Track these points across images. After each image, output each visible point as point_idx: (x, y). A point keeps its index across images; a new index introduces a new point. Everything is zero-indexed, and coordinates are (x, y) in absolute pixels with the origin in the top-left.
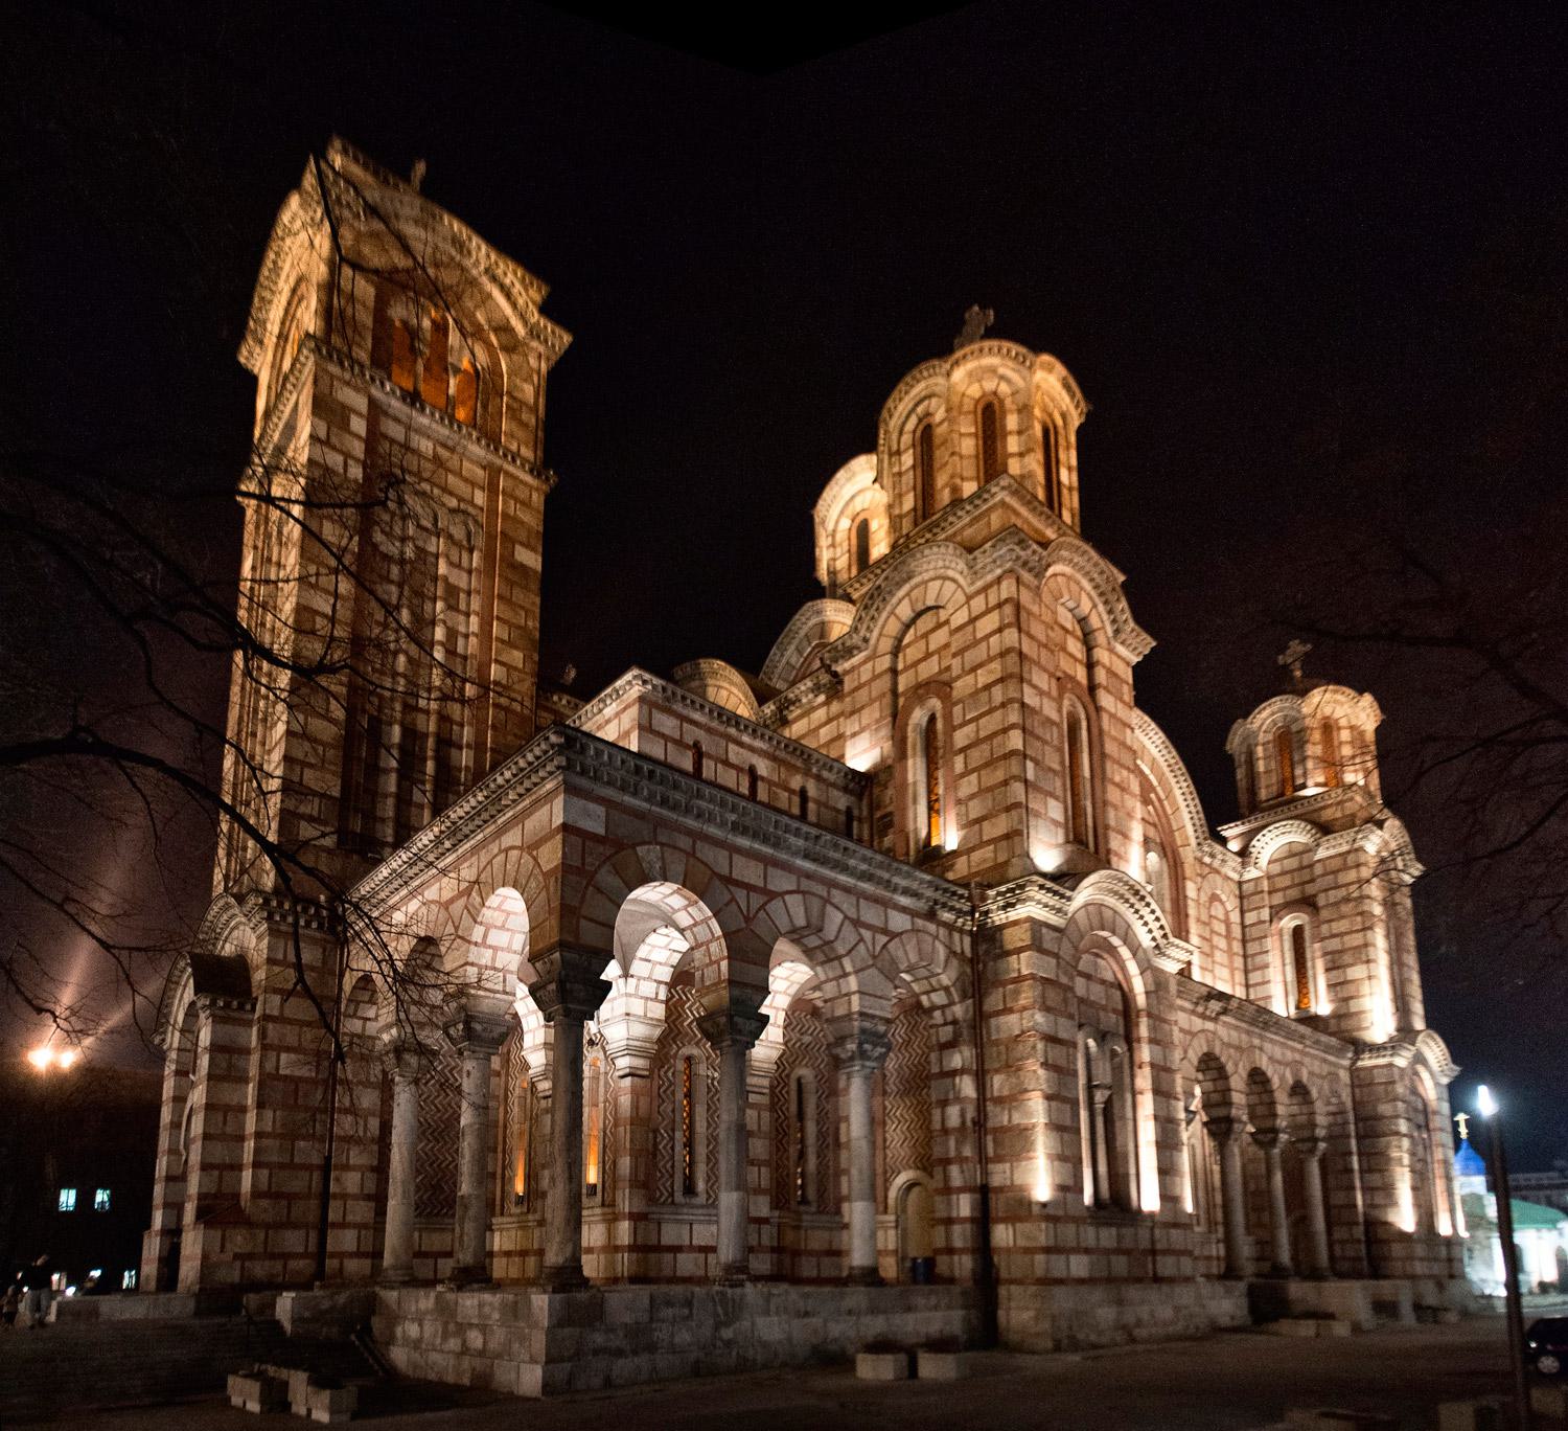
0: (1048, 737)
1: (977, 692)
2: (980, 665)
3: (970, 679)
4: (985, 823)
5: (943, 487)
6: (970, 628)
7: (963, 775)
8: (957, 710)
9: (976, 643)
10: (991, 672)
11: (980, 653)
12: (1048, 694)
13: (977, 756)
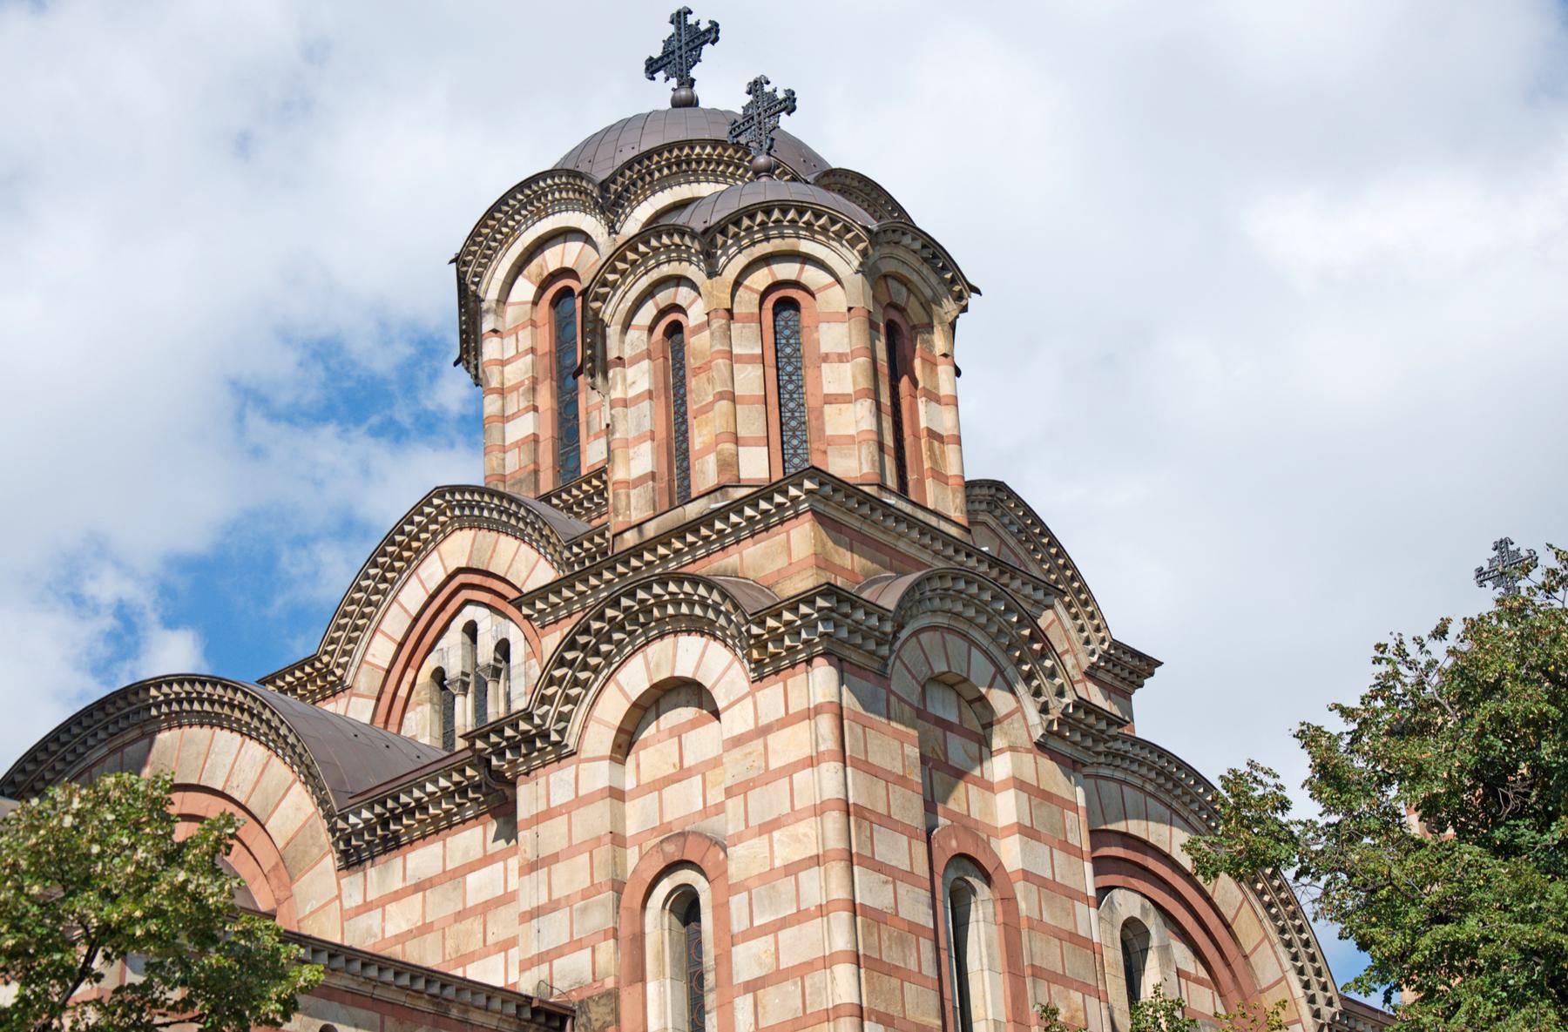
0: (913, 966)
3: (758, 845)
5: (706, 451)
6: (758, 744)
8: (738, 903)
9: (768, 777)
10: (797, 840)
12: (908, 876)
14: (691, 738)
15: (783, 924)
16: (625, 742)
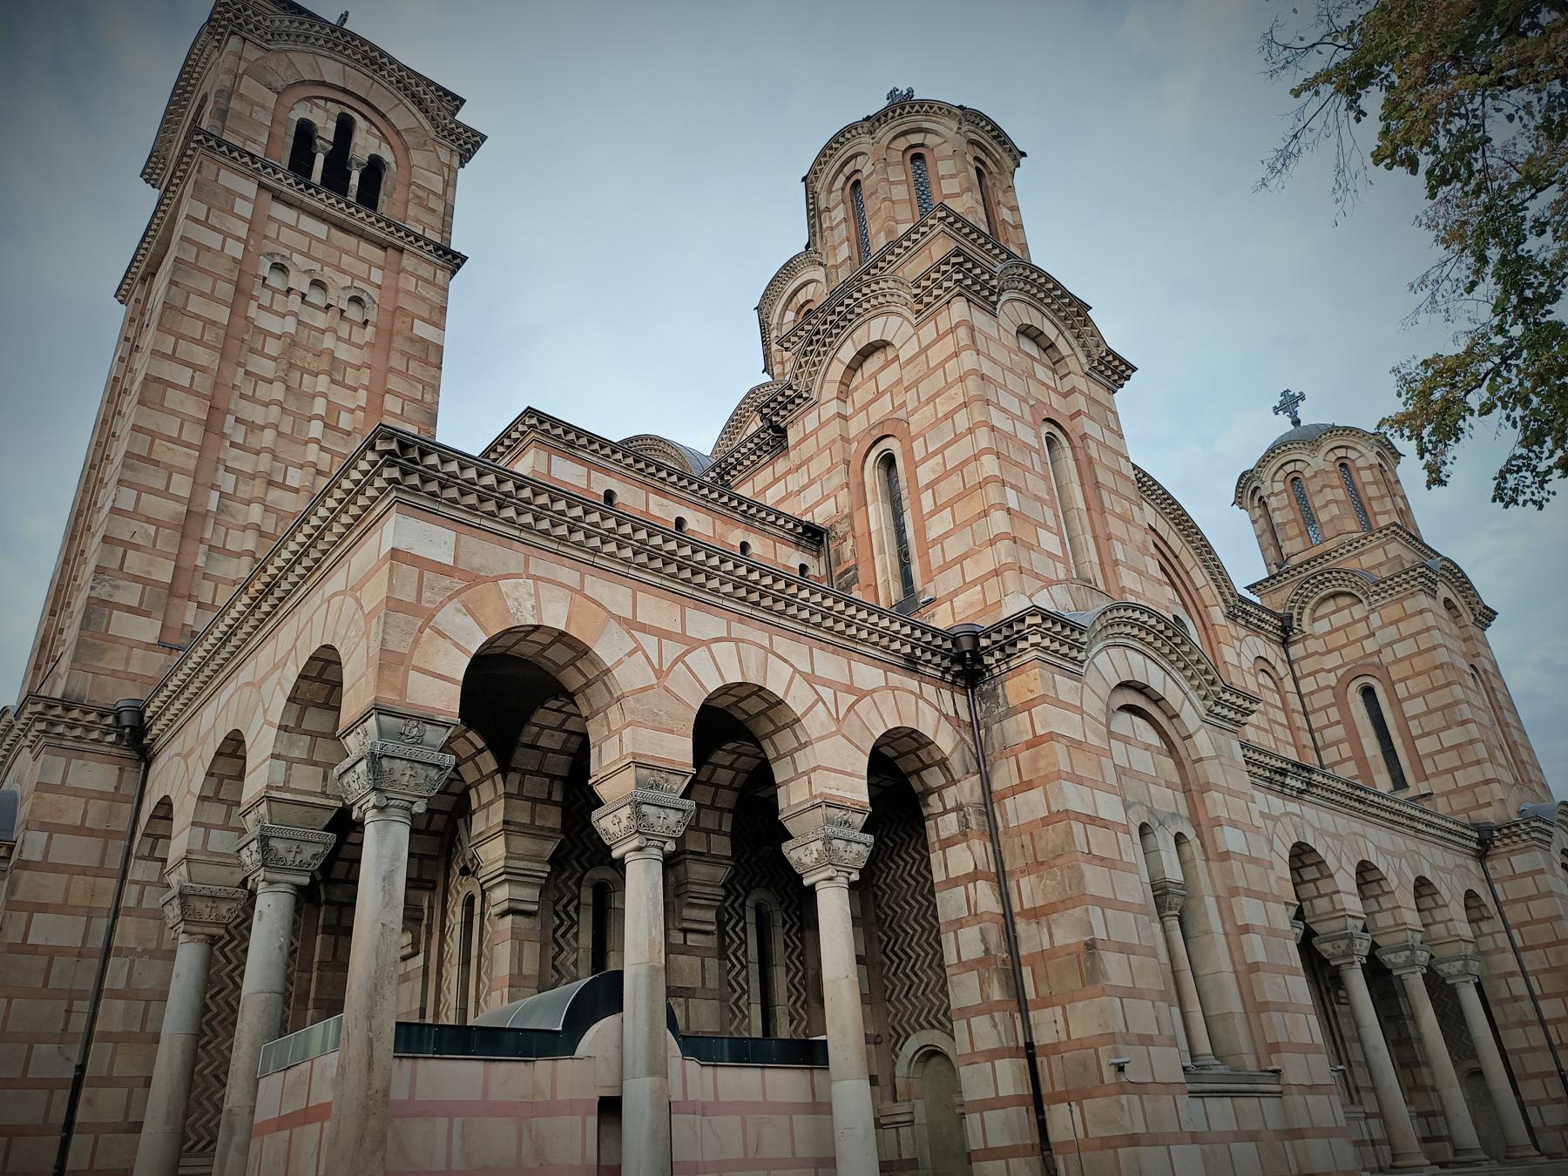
1: (938, 421)
2: (938, 394)
3: (929, 409)
7: (932, 513)
8: (918, 446)
9: (931, 371)
10: (951, 398)
11: (937, 381)
13: (948, 489)
14: (881, 377)
16: (845, 383)
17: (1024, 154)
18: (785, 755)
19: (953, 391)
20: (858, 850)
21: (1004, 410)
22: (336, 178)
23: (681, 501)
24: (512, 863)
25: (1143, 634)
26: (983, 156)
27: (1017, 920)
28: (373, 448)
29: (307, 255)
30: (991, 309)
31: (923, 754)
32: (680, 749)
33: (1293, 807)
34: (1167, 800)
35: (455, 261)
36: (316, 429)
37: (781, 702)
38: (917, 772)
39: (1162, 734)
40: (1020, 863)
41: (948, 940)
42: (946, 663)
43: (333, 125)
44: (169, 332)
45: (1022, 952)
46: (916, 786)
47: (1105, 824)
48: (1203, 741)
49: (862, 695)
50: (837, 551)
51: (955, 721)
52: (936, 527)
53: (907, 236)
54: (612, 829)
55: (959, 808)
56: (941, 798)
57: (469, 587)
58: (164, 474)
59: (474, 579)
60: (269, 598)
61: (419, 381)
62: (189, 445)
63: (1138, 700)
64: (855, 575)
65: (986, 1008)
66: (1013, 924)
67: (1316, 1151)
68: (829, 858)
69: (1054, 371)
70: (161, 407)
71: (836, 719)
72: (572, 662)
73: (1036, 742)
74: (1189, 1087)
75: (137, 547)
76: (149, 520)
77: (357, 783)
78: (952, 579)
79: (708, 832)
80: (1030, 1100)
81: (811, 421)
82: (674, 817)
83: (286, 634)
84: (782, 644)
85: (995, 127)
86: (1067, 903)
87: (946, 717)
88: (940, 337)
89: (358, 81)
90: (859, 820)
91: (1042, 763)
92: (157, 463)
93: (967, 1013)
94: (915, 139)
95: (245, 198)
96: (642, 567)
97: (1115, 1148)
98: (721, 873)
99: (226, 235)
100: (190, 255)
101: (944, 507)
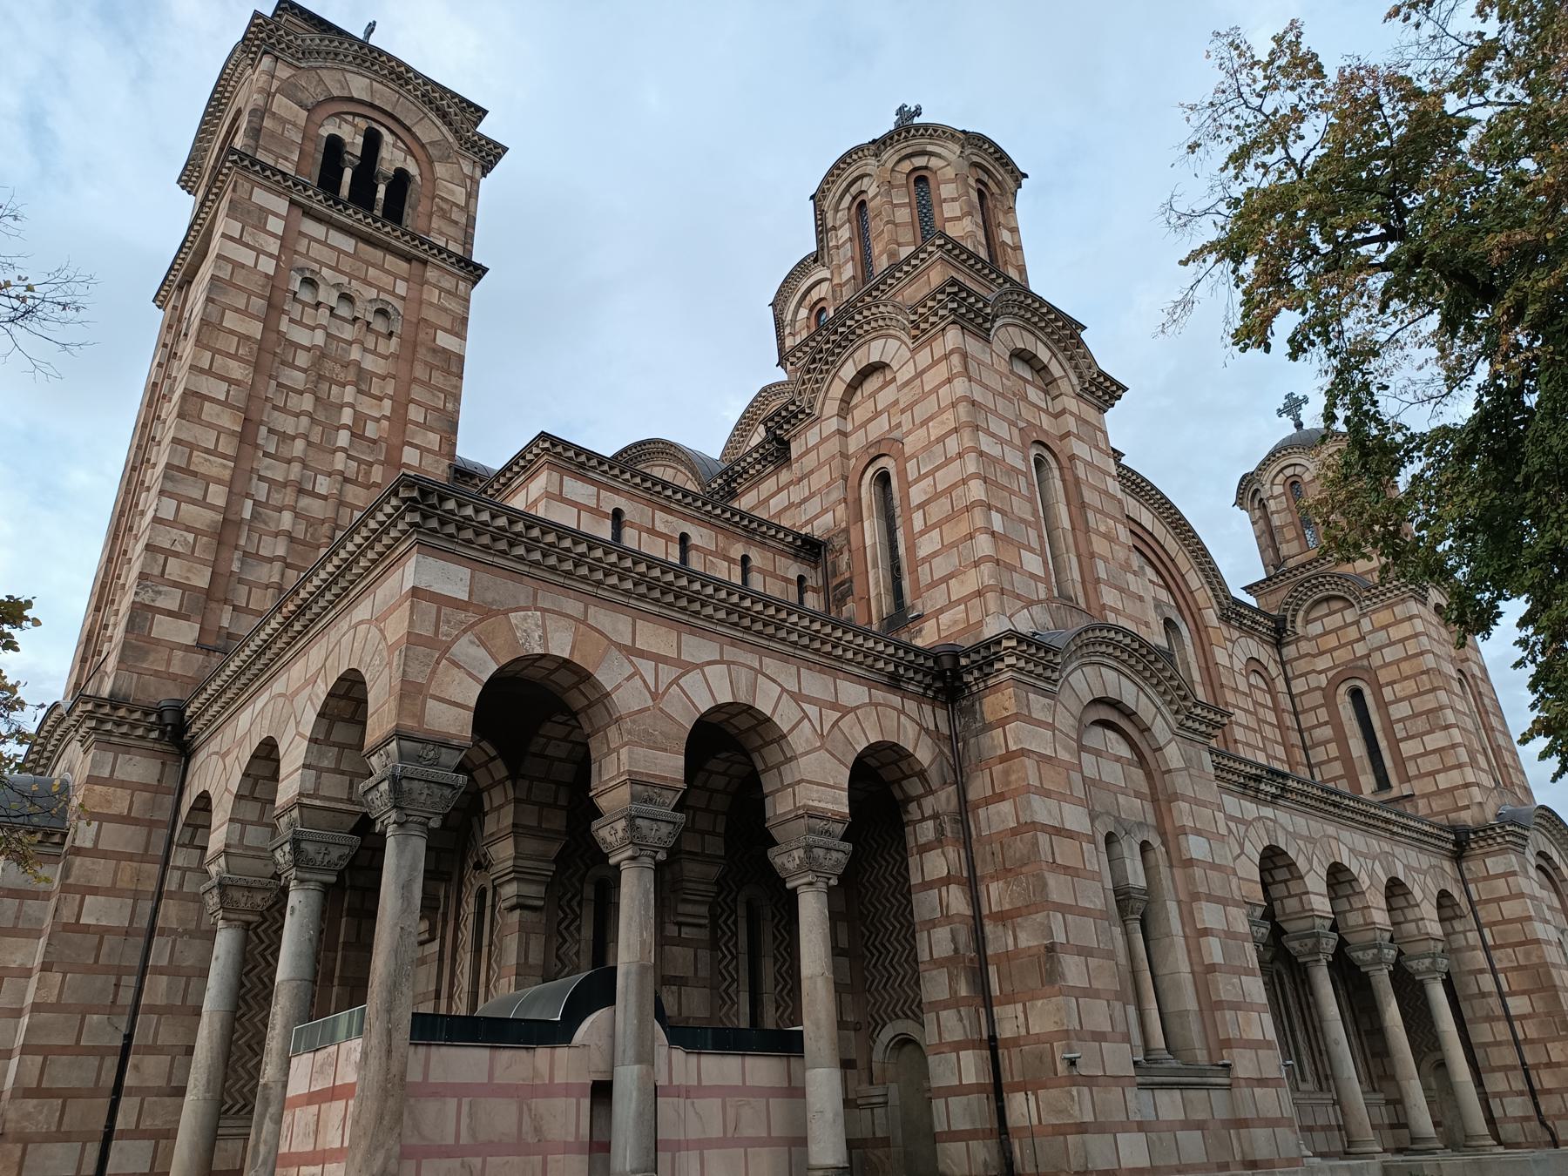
1: (930, 445)
2: (931, 418)
3: (922, 432)
4: (952, 582)
8: (911, 466)
9: (925, 395)
10: (943, 423)
11: (930, 406)
13: (938, 510)
14: (880, 396)
15: (938, 468)
17: (1025, 176)
18: (772, 768)
19: (945, 416)
20: (837, 857)
21: (993, 435)
22: (362, 195)
23: (685, 517)
24: (520, 863)
25: (1118, 653)
26: (985, 178)
27: (986, 922)
28: (396, 495)
29: (336, 269)
30: (985, 336)
31: (904, 765)
32: (671, 765)
33: (1268, 812)
34: (1134, 808)
35: (476, 272)
36: (343, 438)
37: (769, 720)
38: (899, 781)
39: (1133, 746)
40: (990, 870)
41: (922, 937)
42: (928, 680)
43: (360, 140)
44: (206, 347)
45: (989, 952)
46: (898, 795)
47: (1070, 835)
48: (1173, 755)
49: (846, 711)
50: (834, 563)
51: (935, 735)
52: (926, 546)
53: (907, 261)
54: (609, 839)
55: (935, 816)
56: (920, 806)
57: (481, 621)
58: (201, 484)
59: (487, 612)
60: (302, 619)
61: (442, 390)
62: (225, 456)
63: (1110, 714)
64: (850, 588)
65: (954, 1003)
66: (982, 926)
67: (1261, 1142)
68: (810, 864)
69: (1046, 393)
70: (198, 419)
71: (822, 730)
72: (576, 686)
73: (1009, 756)
74: (1139, 1080)
75: (177, 555)
76: (188, 529)
77: (379, 799)
78: (938, 598)
79: (703, 833)
80: (990, 1089)
81: (812, 436)
82: (665, 829)
83: (316, 654)
84: (771, 666)
85: (998, 149)
86: (1029, 909)
87: (927, 730)
88: (935, 363)
89: (385, 96)
90: (839, 829)
91: (1013, 777)
92: (195, 474)
93: (938, 1006)
94: (920, 161)
95: (277, 215)
96: (642, 597)
97: (1065, 1135)
98: (714, 872)
99: (259, 252)
100: (225, 274)
101: (934, 526)
